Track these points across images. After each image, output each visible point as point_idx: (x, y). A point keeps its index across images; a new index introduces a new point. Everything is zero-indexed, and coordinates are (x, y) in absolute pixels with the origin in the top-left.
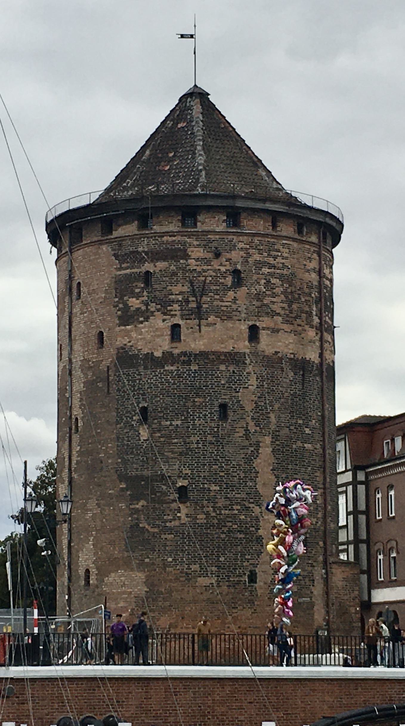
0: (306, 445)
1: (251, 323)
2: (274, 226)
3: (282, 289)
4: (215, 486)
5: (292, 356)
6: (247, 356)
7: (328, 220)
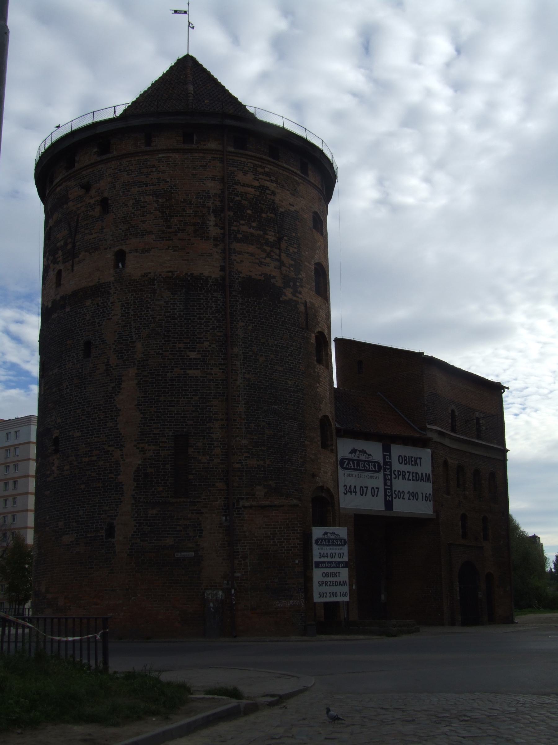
0: (188, 372)
1: (117, 249)
2: (148, 143)
3: (156, 206)
4: (78, 432)
5: (170, 274)
6: (111, 285)
7: (228, 122)
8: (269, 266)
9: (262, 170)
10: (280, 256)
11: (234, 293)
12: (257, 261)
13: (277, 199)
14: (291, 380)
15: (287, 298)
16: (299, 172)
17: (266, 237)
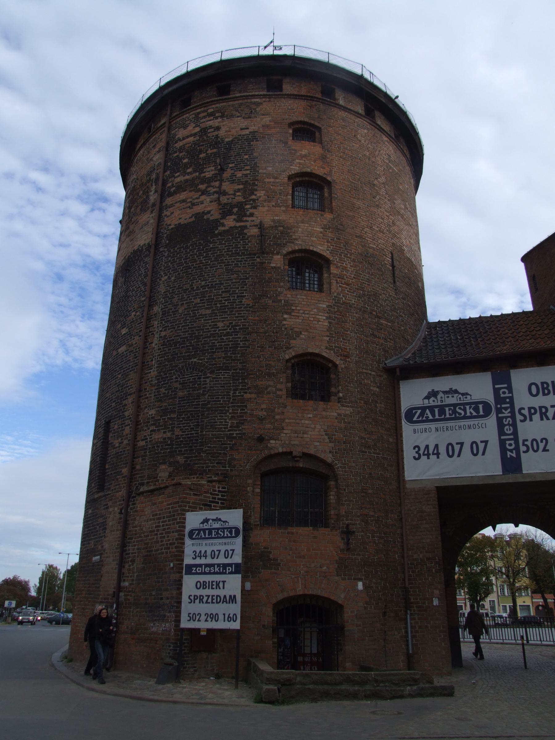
8: (203, 203)
9: (205, 114)
10: (220, 187)
11: (161, 249)
12: (189, 204)
13: (222, 133)
14: (223, 321)
15: (227, 228)
17: (203, 175)
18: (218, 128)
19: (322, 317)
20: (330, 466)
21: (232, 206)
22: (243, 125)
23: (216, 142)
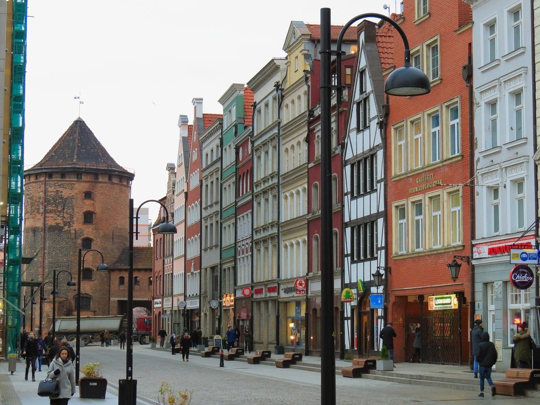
13: (63, 194)
16: (76, 179)
18: (62, 192)
19: (91, 257)
20: (91, 296)
21: (67, 223)
22: (70, 192)
23: (62, 198)
